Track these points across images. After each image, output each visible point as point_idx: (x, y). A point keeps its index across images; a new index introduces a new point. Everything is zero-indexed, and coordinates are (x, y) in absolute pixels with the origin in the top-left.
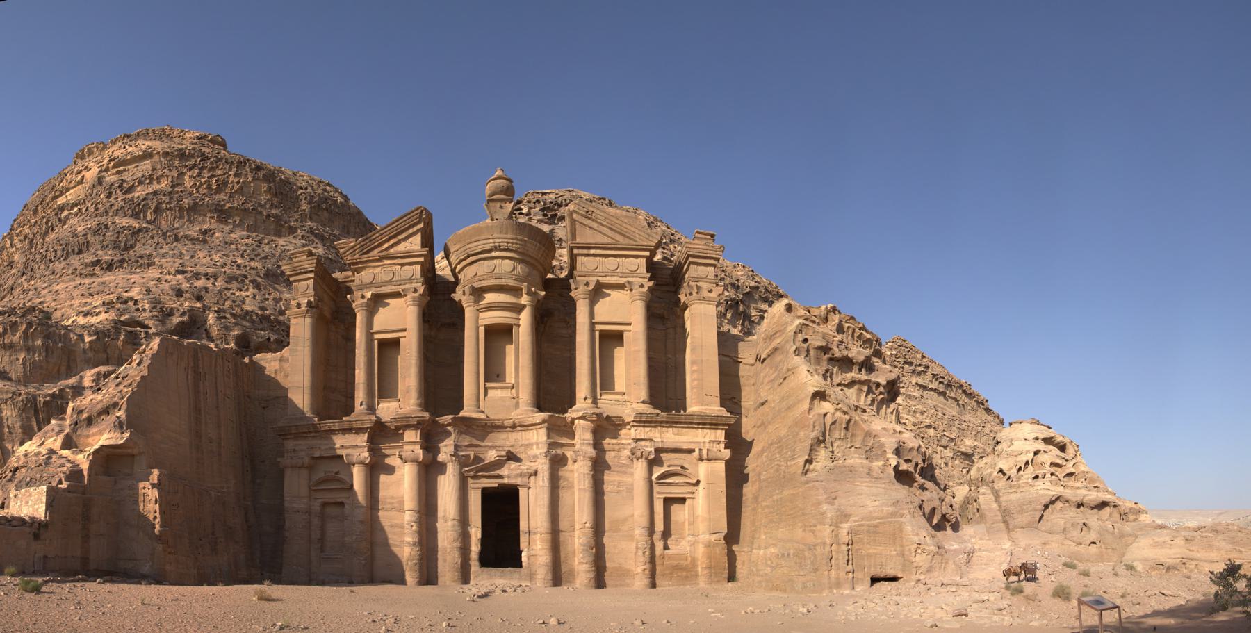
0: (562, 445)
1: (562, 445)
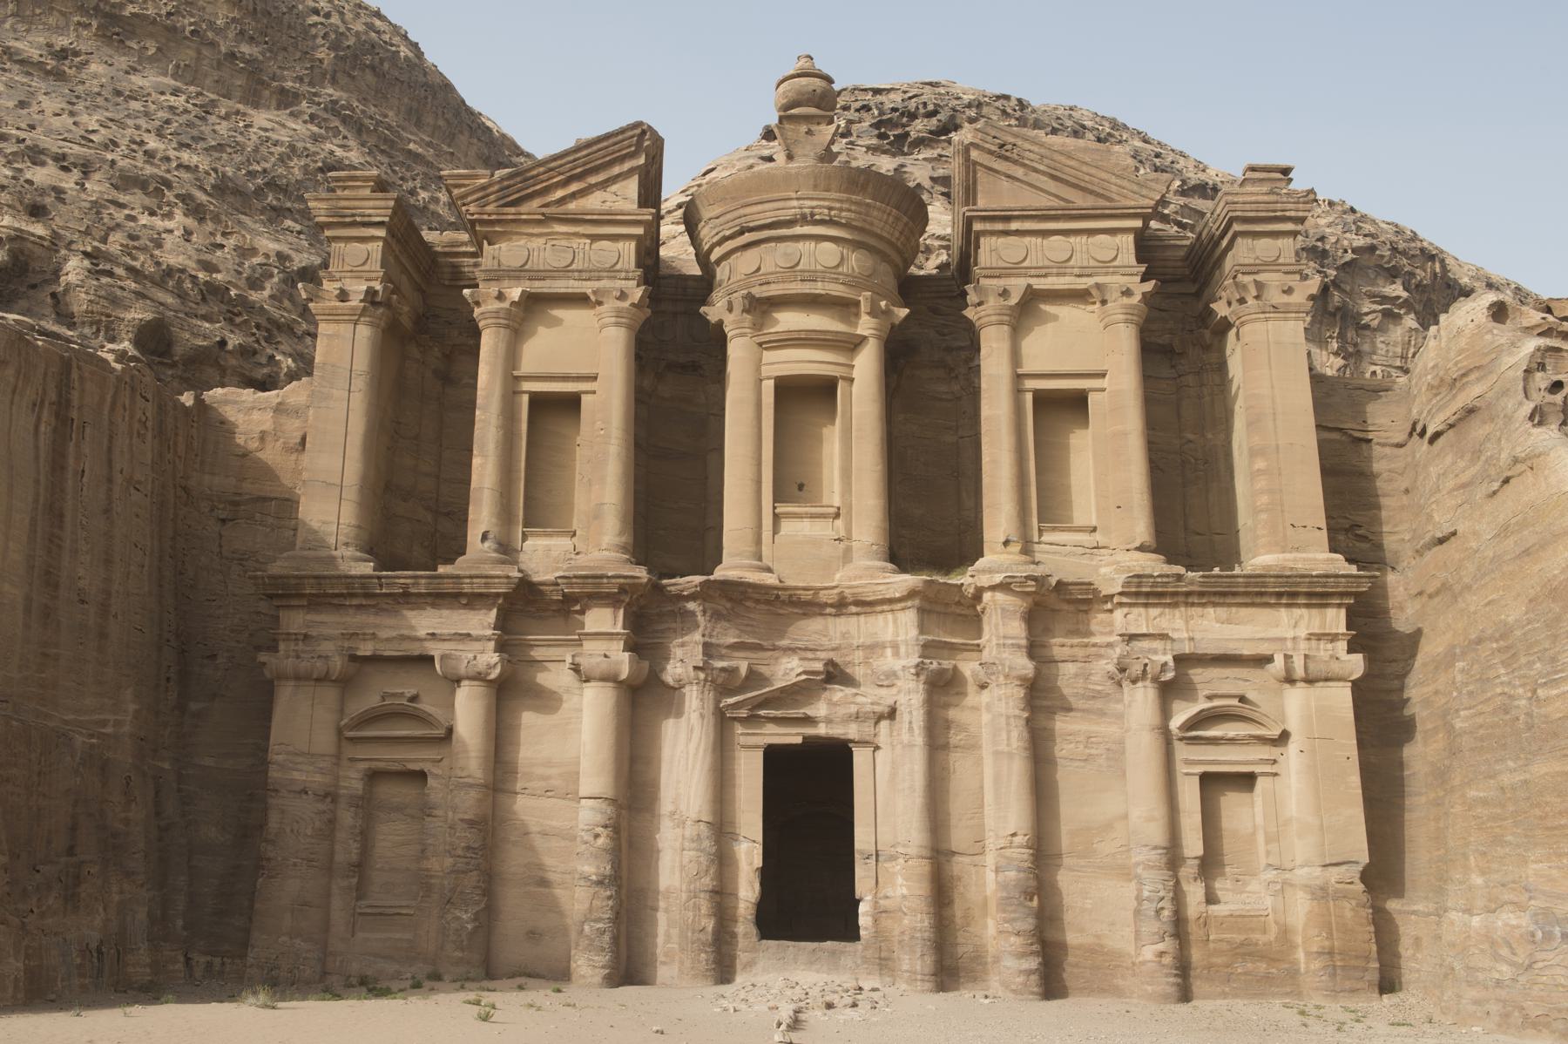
1: (952, 648)
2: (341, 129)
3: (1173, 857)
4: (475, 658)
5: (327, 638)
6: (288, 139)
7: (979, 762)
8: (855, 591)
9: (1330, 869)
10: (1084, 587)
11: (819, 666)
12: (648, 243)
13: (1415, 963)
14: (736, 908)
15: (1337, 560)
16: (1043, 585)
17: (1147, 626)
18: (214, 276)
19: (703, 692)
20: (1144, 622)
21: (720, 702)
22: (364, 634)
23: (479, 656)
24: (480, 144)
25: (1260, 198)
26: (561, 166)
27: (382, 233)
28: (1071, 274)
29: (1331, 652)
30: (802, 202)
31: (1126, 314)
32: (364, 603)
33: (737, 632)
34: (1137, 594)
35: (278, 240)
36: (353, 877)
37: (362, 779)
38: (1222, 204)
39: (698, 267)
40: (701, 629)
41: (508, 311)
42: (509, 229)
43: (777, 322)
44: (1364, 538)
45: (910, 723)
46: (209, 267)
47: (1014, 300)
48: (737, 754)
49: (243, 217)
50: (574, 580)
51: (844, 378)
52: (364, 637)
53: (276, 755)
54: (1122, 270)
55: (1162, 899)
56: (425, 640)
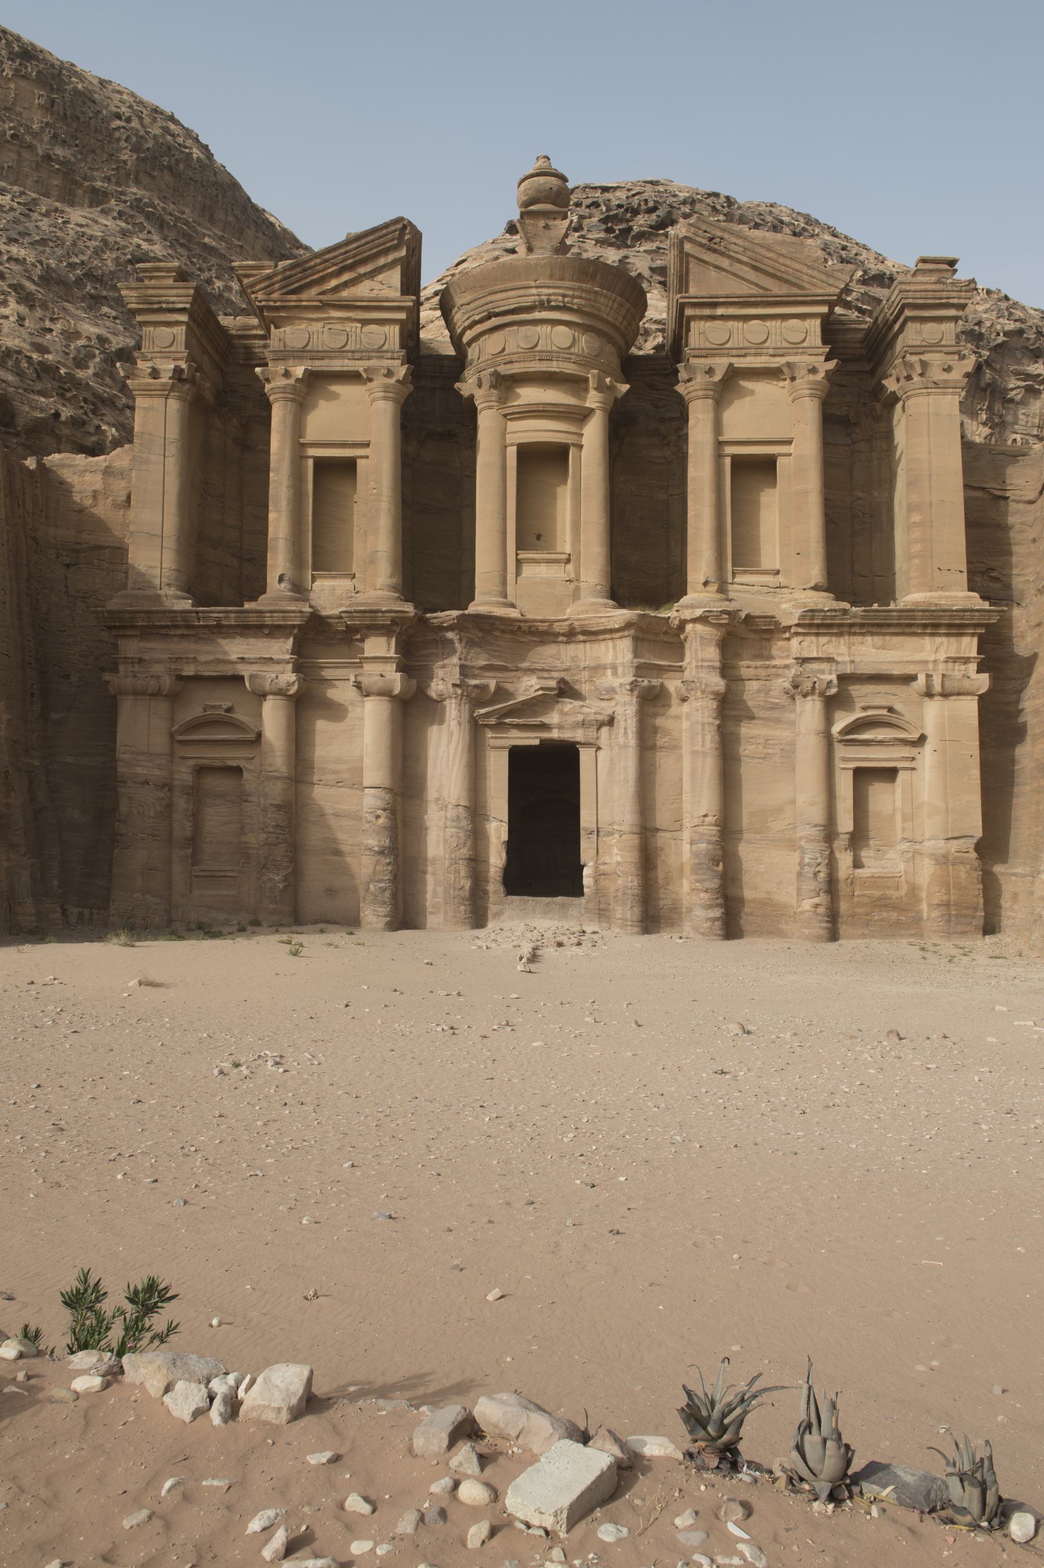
0: (661, 670)
2: (145, 225)
3: (829, 832)
4: (277, 677)
5: (159, 662)
6: (101, 234)
7: (679, 760)
8: (583, 623)
9: (952, 841)
10: (768, 620)
11: (553, 684)
12: (410, 326)
13: (1012, 912)
14: (488, 871)
15: (974, 597)
16: (734, 618)
17: (817, 652)
18: (46, 356)
19: (460, 705)
20: (815, 648)
21: (474, 712)
22: (187, 658)
23: (280, 676)
24: (264, 238)
25: (929, 287)
26: (335, 257)
27: (184, 318)
28: (767, 354)
29: (963, 672)
30: (540, 290)
31: (811, 389)
32: (186, 633)
33: (487, 656)
34: (810, 625)
35: (97, 325)
36: (189, 848)
37: (192, 773)
38: (896, 292)
39: (452, 348)
40: (458, 654)
41: (294, 387)
42: (292, 314)
43: (519, 396)
44: (996, 579)
45: (626, 729)
46: (42, 349)
47: (718, 377)
48: (487, 753)
49: (67, 304)
50: (355, 614)
51: (574, 445)
52: (188, 661)
53: (123, 754)
54: (810, 351)
55: (819, 864)
56: (236, 663)
